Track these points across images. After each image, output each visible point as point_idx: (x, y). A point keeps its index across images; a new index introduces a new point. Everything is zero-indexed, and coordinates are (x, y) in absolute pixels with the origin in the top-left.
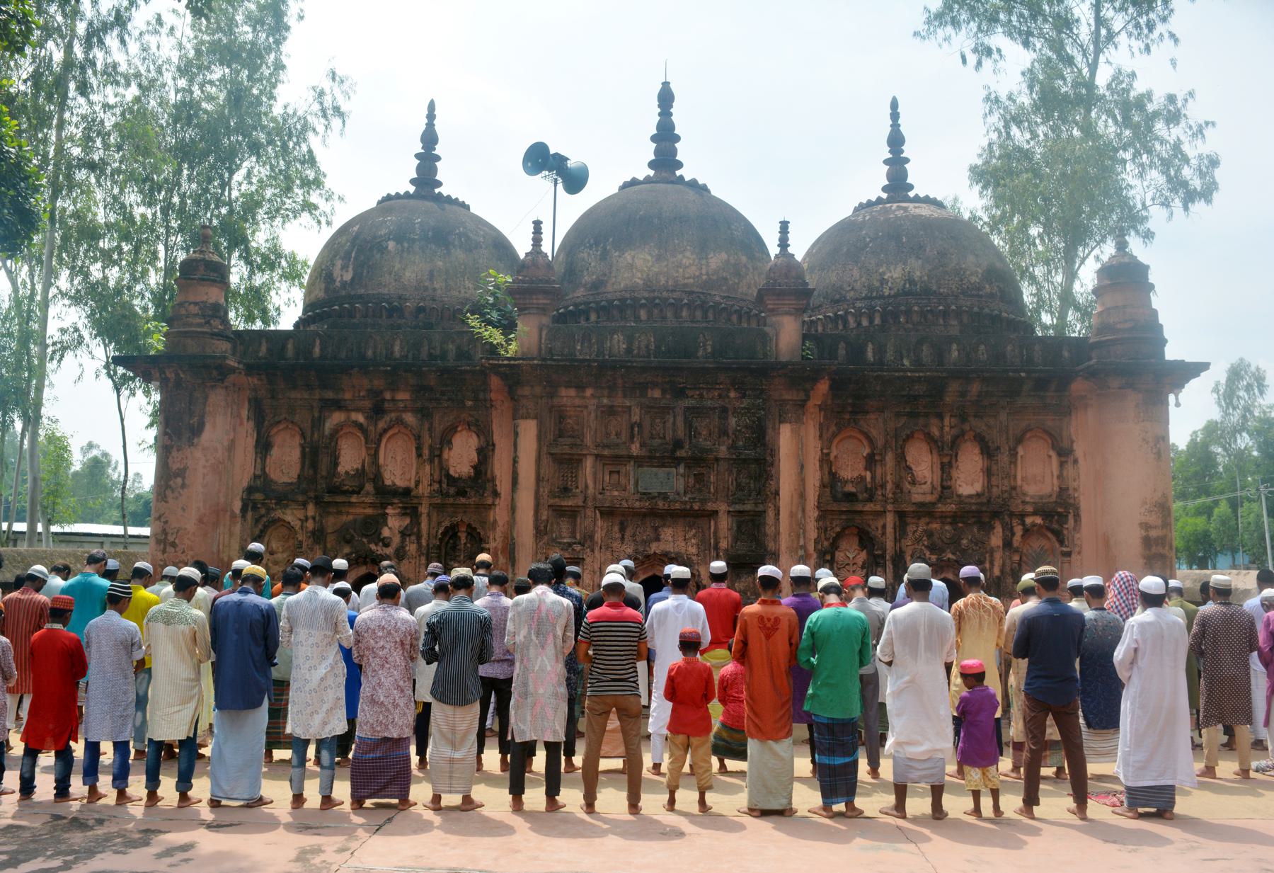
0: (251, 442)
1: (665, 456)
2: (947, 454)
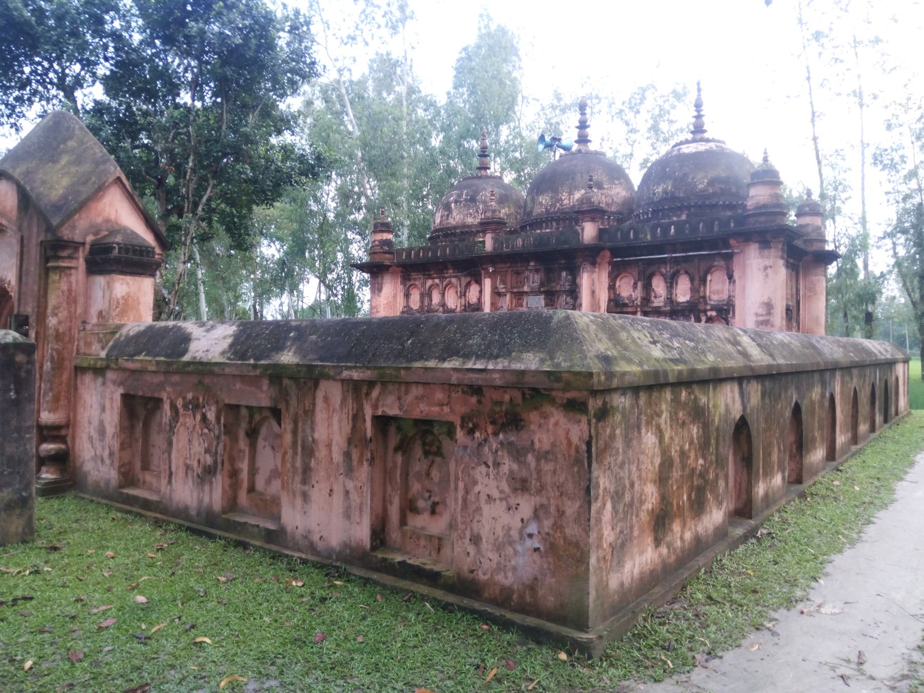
0: (402, 294)
2: (671, 282)
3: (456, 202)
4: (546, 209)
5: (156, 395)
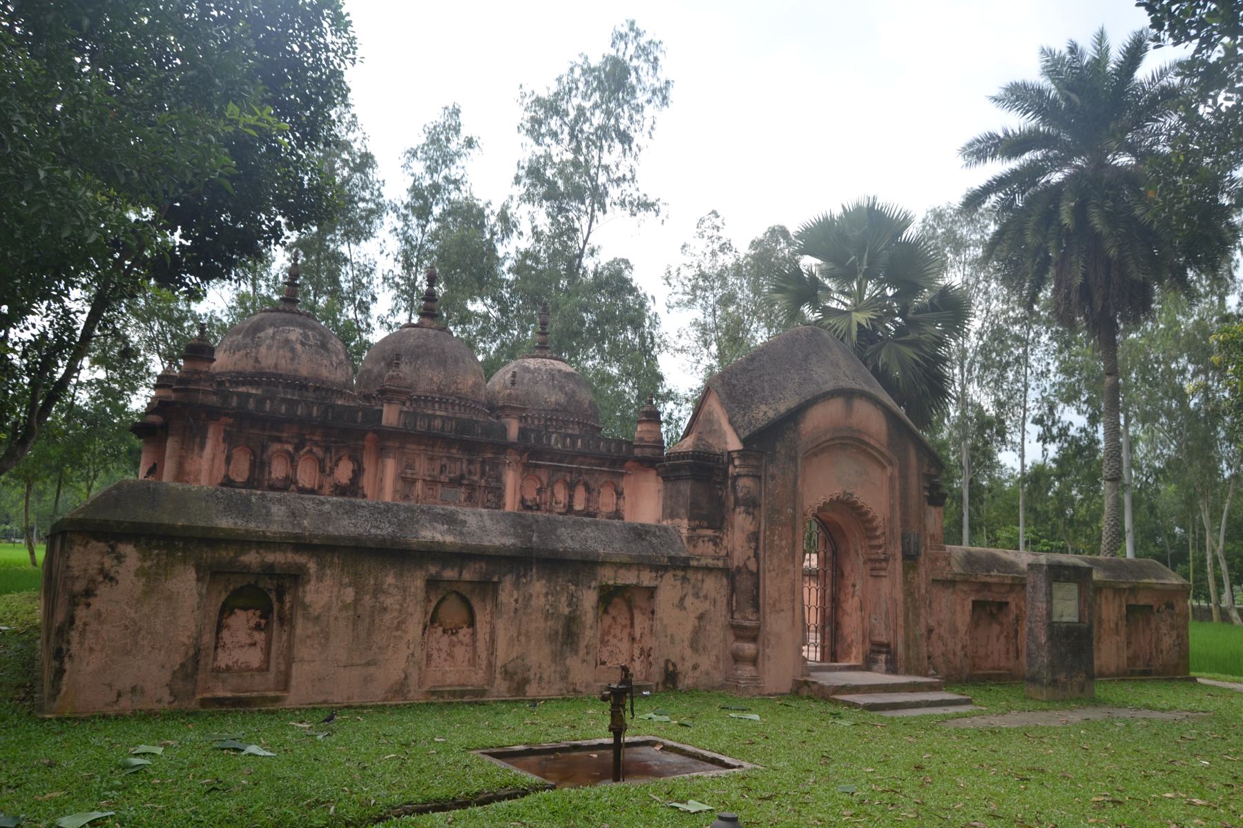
1: (456, 482)
2: (571, 487)
3: (303, 344)
4: (439, 388)
5: (1004, 600)
